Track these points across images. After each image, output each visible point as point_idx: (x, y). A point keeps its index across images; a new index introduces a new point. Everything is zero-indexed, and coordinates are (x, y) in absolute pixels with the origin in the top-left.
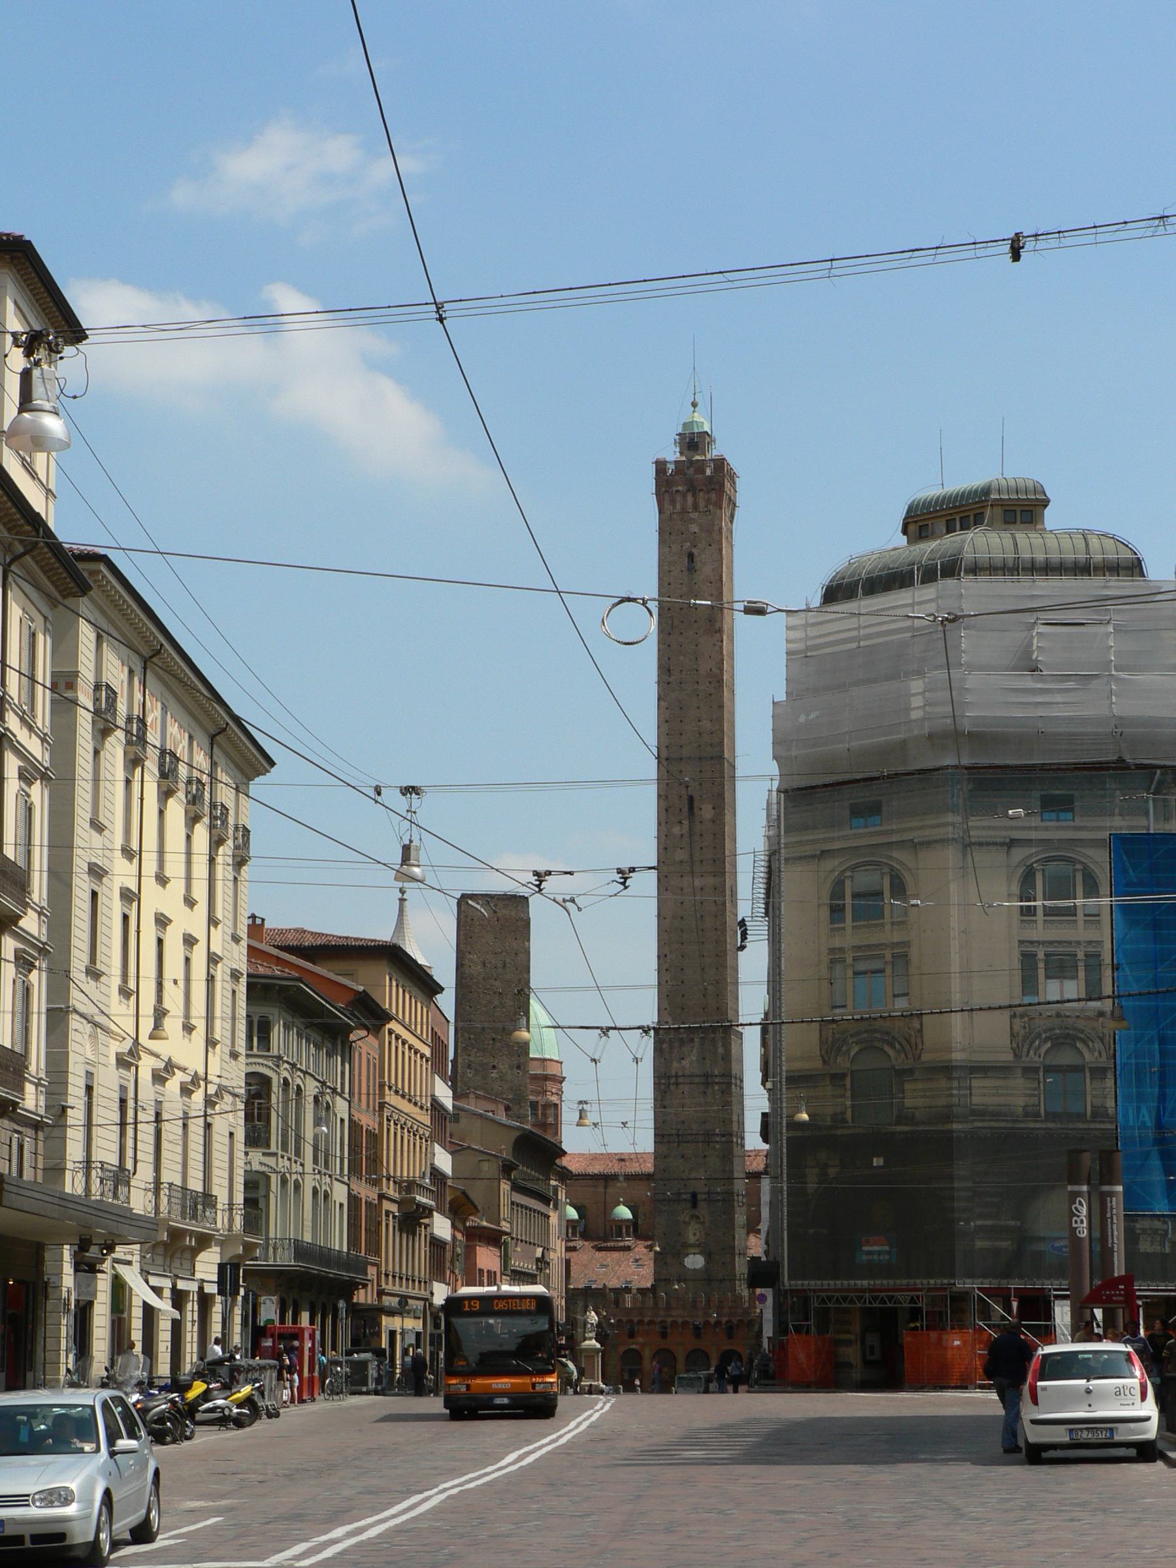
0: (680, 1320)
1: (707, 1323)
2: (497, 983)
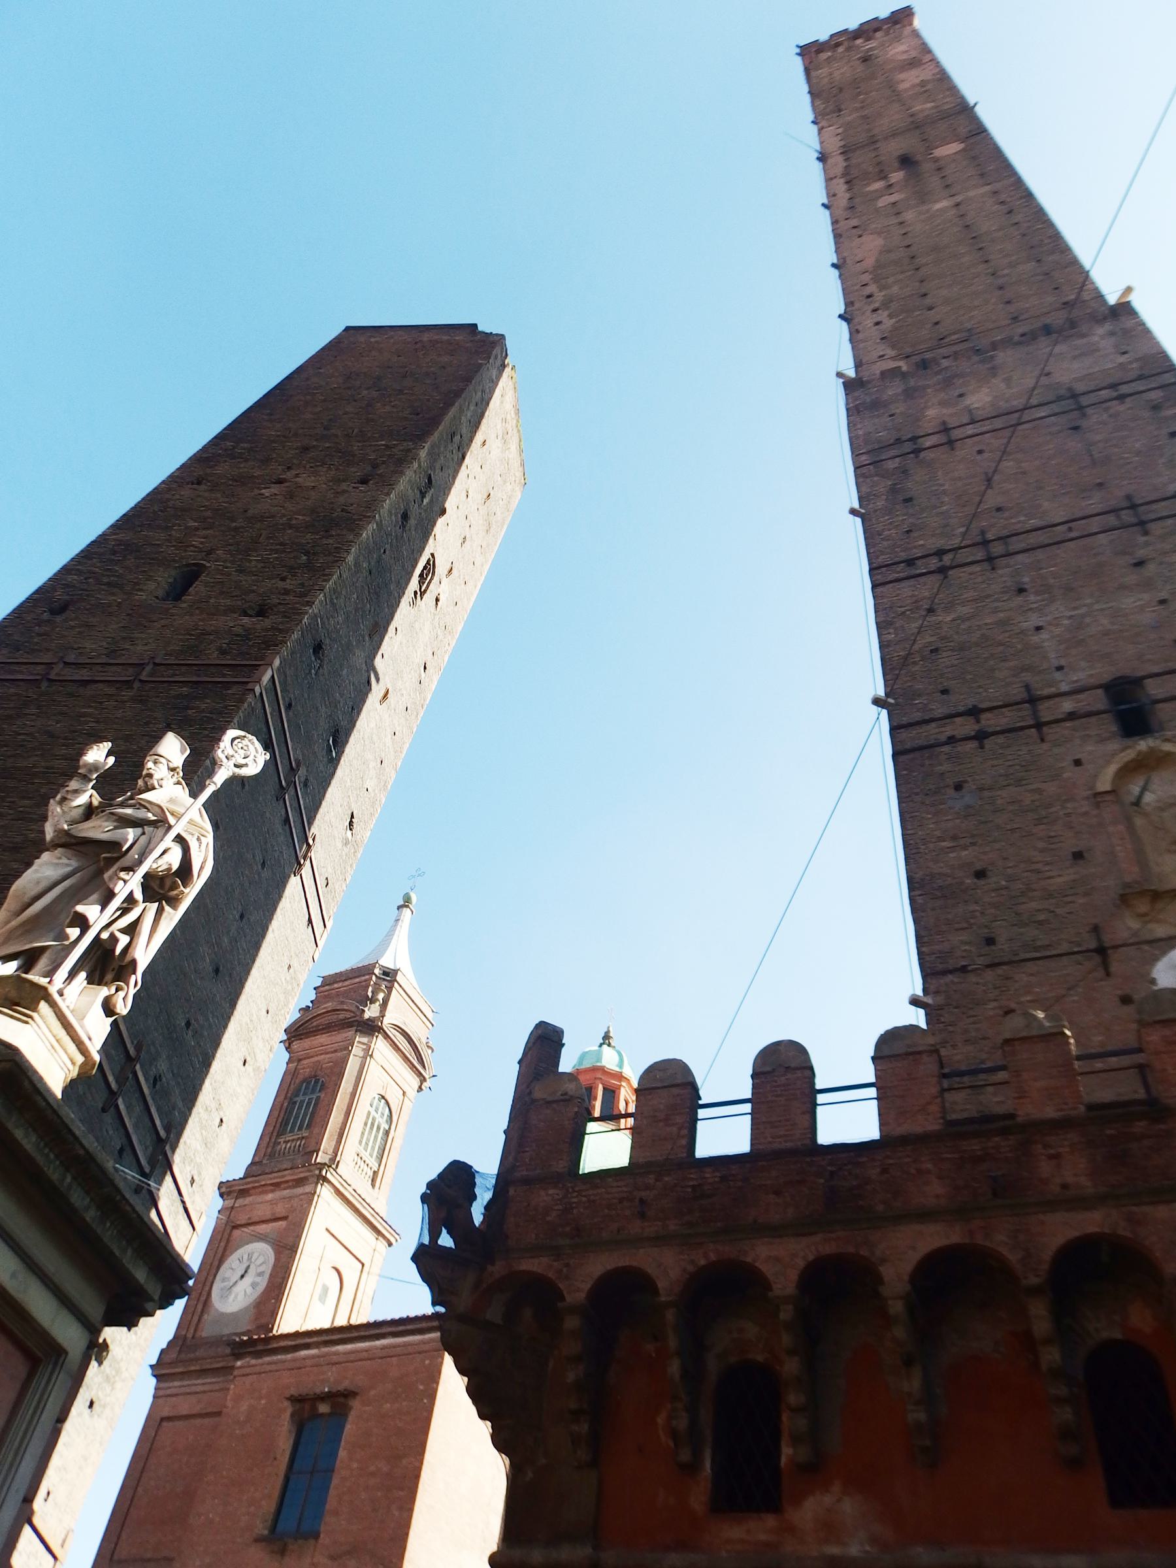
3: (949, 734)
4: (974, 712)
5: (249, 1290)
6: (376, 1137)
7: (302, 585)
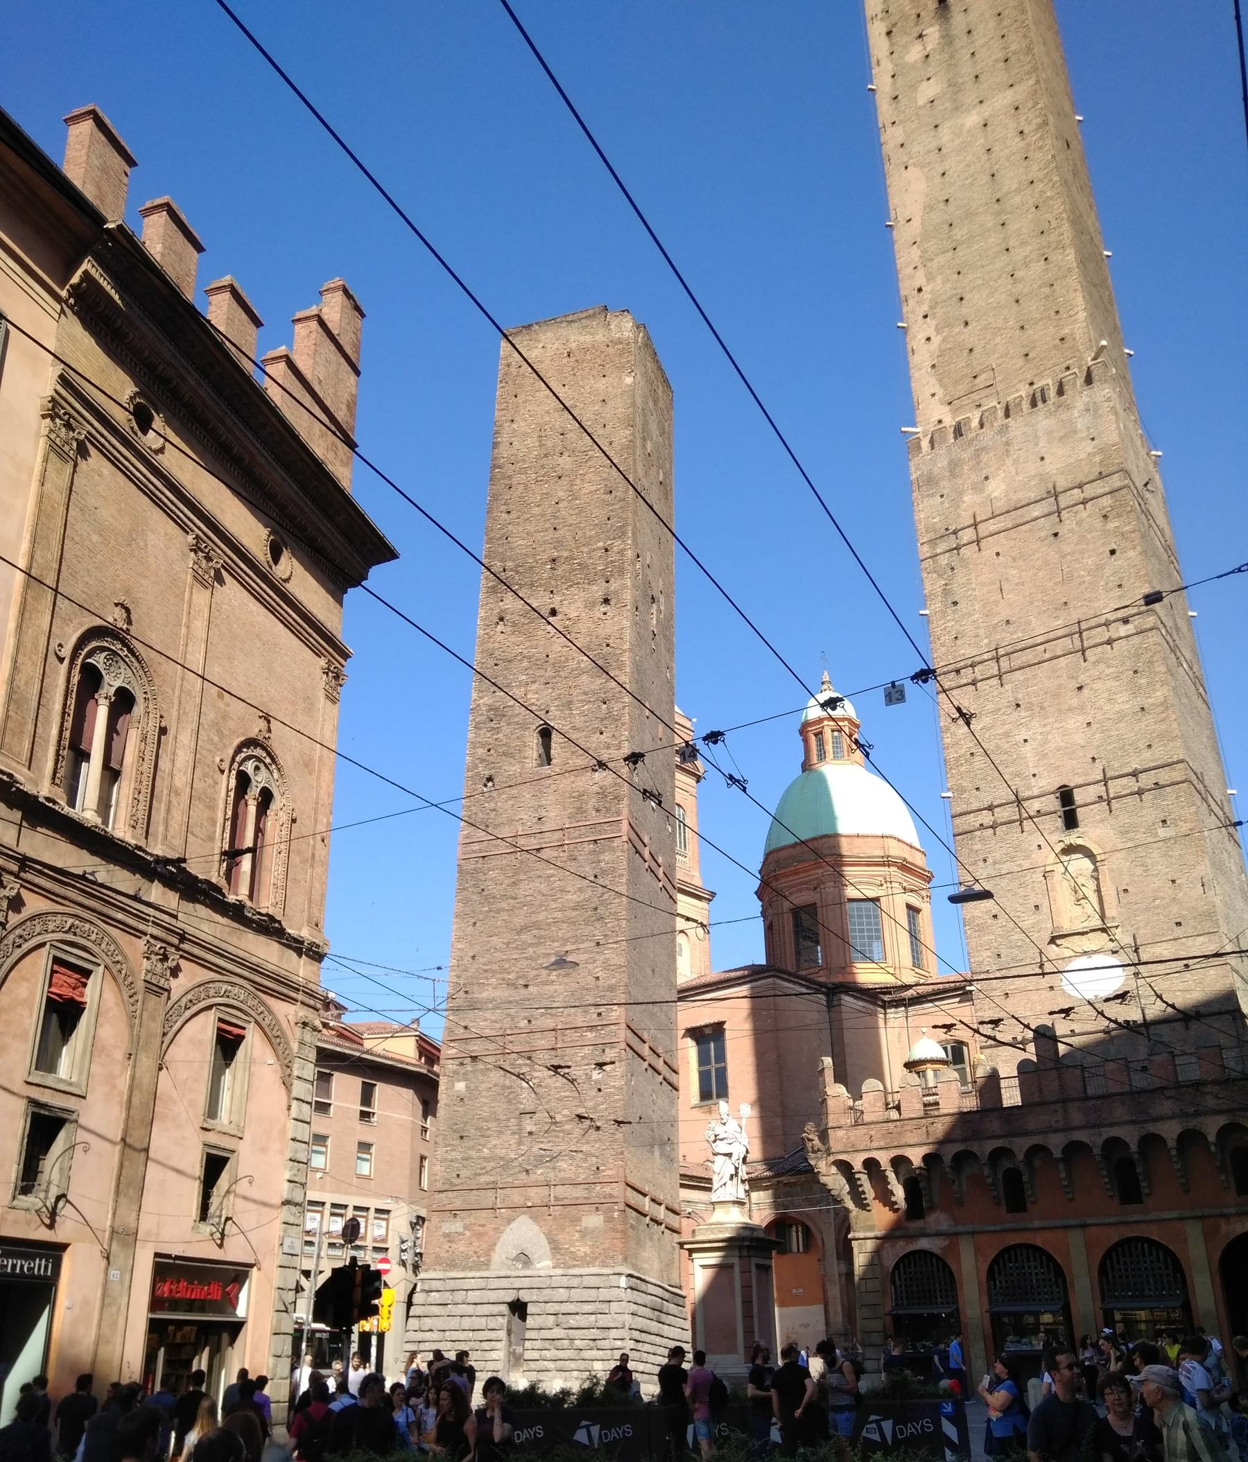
0: (1056, 1143)
1: (1151, 1141)
2: (561, 461)
3: (980, 822)
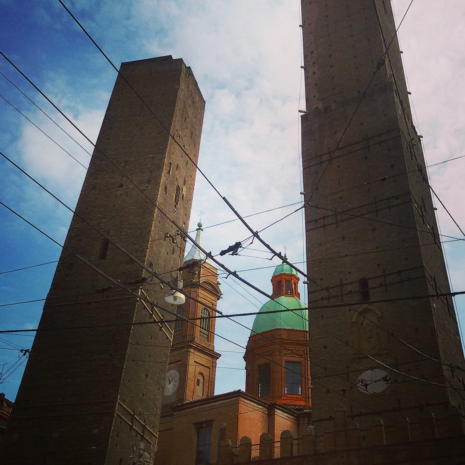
4: (327, 289)
5: (173, 387)
6: (206, 323)
7: (141, 246)
